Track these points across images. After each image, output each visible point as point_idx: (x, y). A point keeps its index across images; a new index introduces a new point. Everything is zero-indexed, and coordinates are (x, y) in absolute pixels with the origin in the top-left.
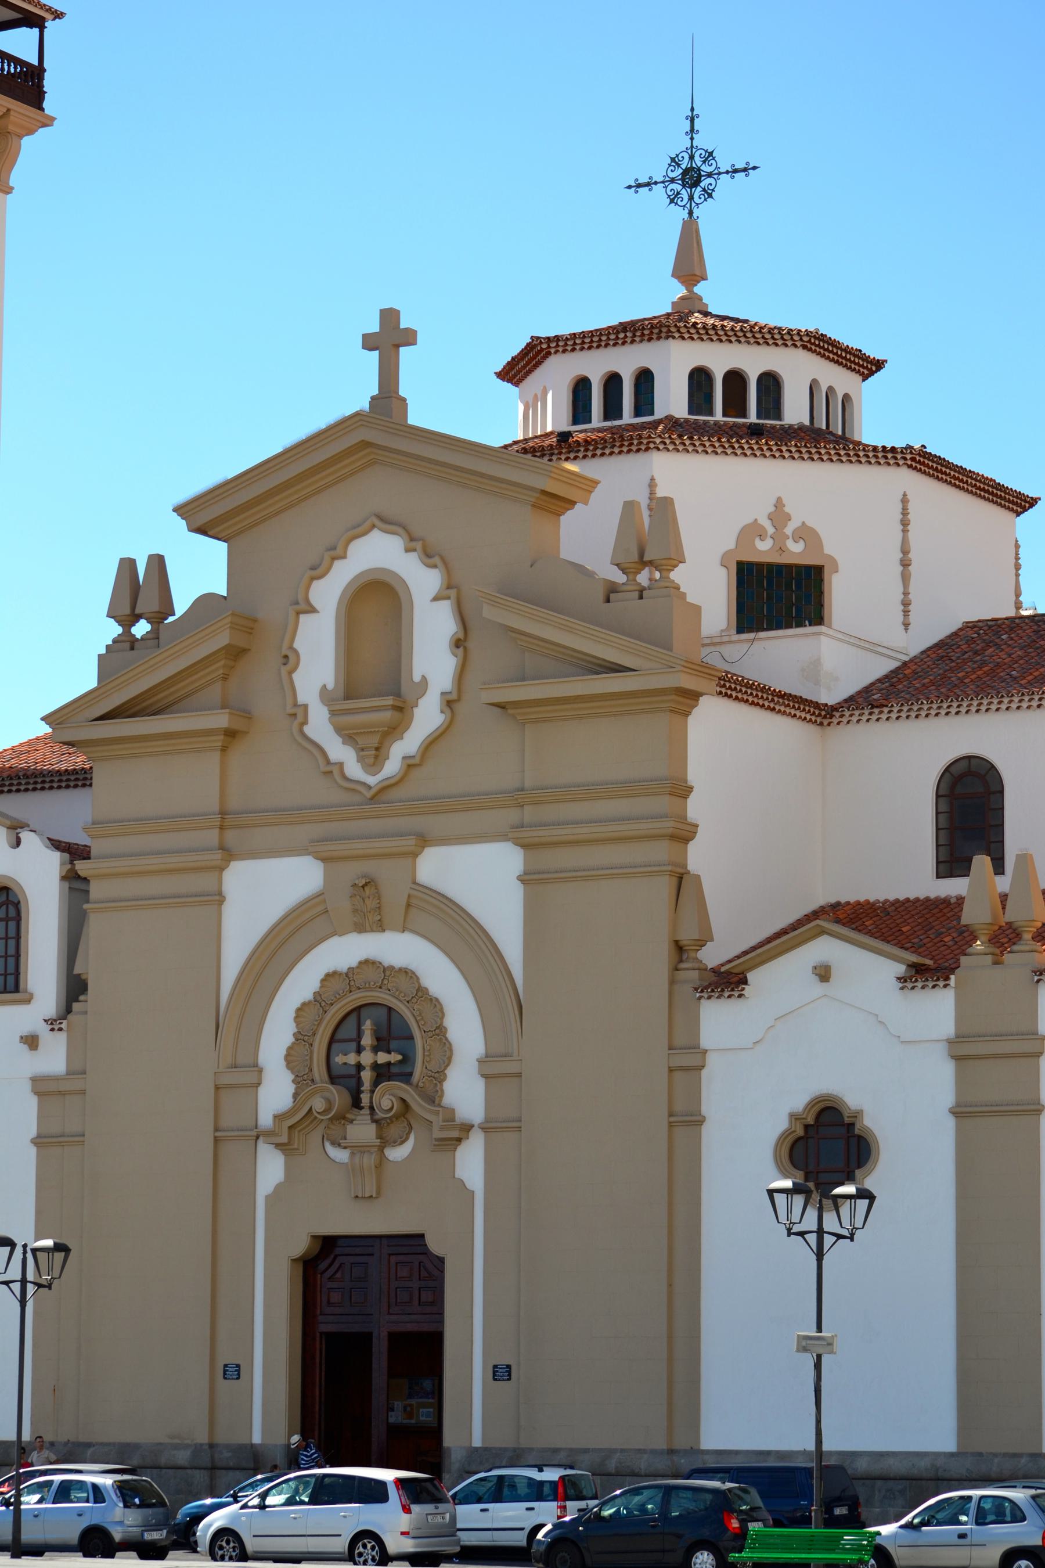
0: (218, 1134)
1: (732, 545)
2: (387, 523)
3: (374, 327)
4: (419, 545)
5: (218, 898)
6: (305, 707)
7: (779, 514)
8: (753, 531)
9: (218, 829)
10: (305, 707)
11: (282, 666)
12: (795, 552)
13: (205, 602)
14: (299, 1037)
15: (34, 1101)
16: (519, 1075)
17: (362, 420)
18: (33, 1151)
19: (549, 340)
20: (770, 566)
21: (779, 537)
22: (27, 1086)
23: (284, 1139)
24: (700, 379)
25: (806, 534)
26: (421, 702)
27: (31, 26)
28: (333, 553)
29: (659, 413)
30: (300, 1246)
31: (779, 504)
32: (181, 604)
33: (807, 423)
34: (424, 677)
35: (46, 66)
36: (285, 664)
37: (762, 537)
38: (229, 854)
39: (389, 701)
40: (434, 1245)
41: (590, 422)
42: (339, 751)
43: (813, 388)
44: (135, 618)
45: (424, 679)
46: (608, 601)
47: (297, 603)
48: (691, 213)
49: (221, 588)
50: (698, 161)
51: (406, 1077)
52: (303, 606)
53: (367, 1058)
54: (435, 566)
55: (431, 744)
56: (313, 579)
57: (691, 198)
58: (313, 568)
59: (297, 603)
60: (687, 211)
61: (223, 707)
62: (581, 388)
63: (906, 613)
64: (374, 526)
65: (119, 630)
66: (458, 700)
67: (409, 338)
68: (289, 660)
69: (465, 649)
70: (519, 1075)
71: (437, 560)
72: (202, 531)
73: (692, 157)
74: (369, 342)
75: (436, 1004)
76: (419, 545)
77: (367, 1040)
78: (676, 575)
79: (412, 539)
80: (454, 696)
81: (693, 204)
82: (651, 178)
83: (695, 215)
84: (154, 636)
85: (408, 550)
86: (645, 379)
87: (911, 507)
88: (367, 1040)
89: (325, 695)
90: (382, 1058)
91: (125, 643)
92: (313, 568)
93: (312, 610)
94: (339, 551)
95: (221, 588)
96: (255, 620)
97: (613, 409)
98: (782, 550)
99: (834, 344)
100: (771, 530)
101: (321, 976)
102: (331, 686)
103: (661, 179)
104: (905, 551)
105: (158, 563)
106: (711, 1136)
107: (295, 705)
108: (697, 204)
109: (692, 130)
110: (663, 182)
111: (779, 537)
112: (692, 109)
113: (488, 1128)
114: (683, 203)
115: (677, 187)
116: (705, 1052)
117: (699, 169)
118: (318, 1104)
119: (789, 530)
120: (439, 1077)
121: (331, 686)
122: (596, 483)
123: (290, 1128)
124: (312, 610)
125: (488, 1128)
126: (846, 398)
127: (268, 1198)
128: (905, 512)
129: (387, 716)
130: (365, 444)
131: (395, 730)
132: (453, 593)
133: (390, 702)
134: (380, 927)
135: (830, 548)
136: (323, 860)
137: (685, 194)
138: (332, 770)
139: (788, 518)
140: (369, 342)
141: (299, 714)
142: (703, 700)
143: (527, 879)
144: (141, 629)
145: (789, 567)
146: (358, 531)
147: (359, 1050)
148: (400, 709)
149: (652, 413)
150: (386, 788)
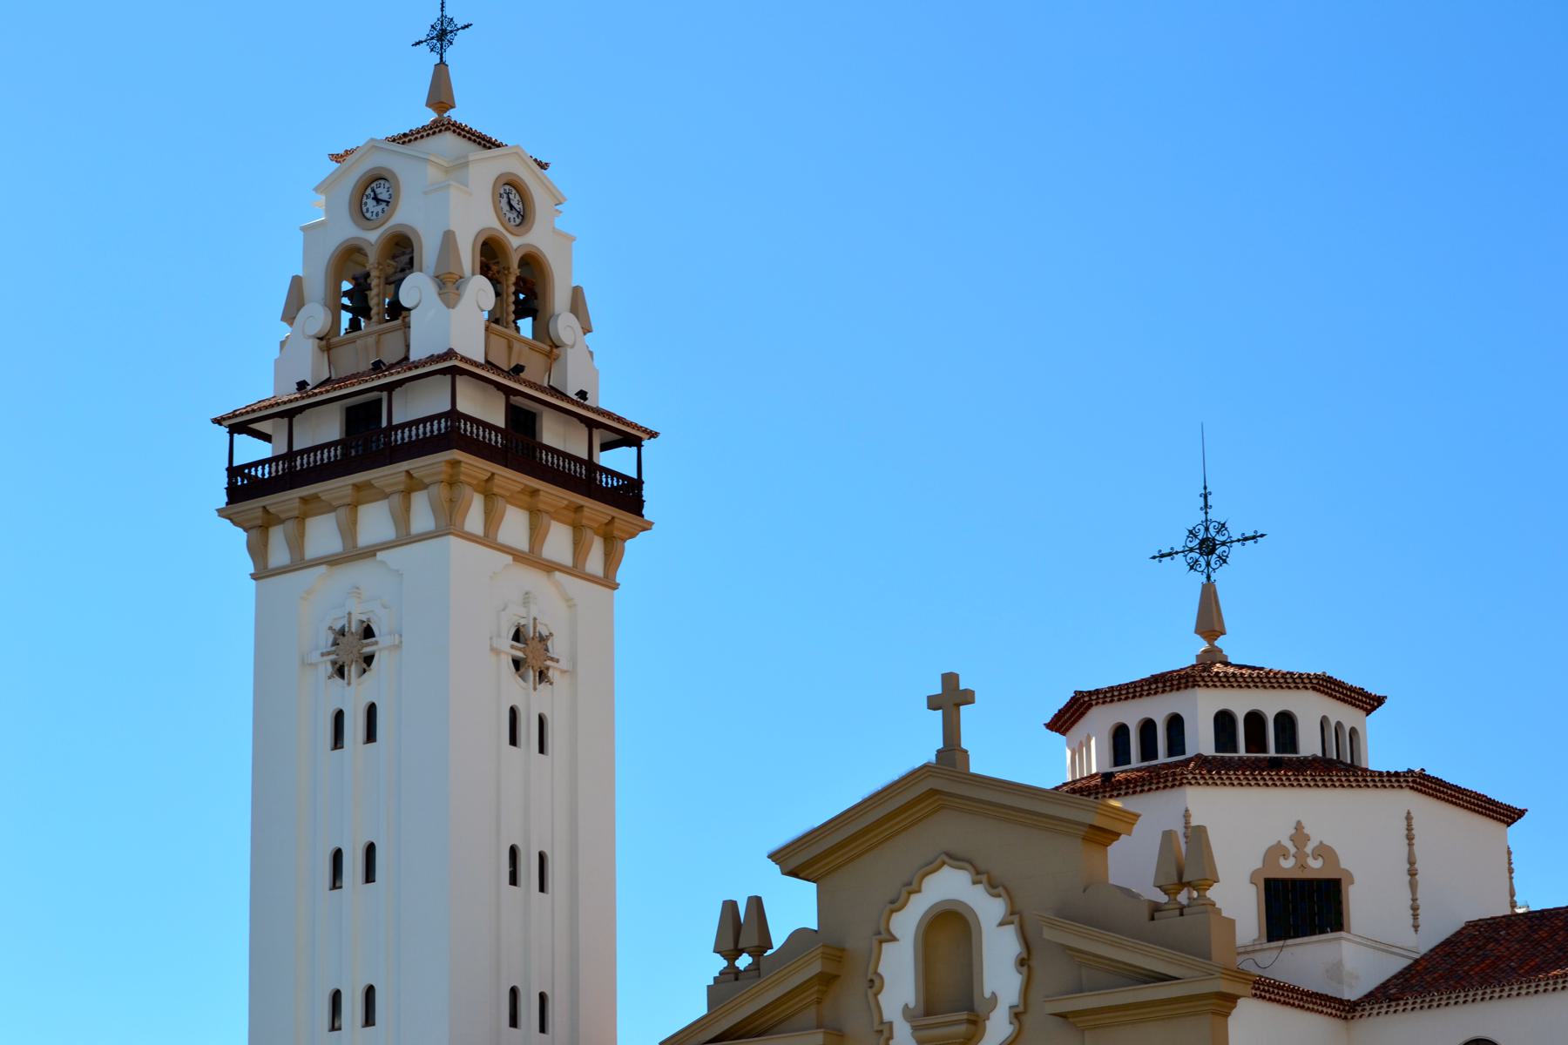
1: (1259, 865)
2: (957, 859)
3: (937, 689)
4: (984, 878)
6: (891, 1024)
7: (1299, 836)
8: (1277, 851)
12: (1316, 867)
13: (799, 936)
19: (1090, 693)
20: (1294, 881)
21: (1300, 856)
24: (1224, 721)
25: (1324, 851)
27: (630, 445)
28: (909, 888)
29: (1190, 753)
31: (1299, 826)
32: (778, 938)
33: (1320, 754)
34: (993, 993)
35: (644, 478)
36: (871, 987)
37: (1285, 856)
39: (964, 1016)
41: (1129, 763)
43: (1324, 722)
44: (738, 953)
45: (993, 993)
46: (1153, 918)
47: (879, 933)
48: (1209, 577)
49: (812, 924)
50: (1212, 532)
52: (882, 937)
54: (999, 896)
56: (893, 911)
57: (1208, 564)
58: (892, 902)
59: (879, 933)
60: (1205, 576)
61: (818, 1027)
62: (1120, 733)
63: (1415, 916)
64: (944, 863)
65: (724, 963)
66: (1024, 1012)
67: (968, 697)
68: (874, 983)
69: (1029, 968)
71: (1000, 890)
72: (794, 873)
73: (1207, 529)
74: (933, 703)
76: (984, 878)
78: (1212, 894)
79: (978, 873)
80: (1021, 1009)
81: (1211, 569)
82: (1172, 549)
83: (1212, 579)
84: (755, 968)
85: (975, 883)
86: (1176, 723)
87: (1414, 822)
91: (731, 974)
92: (892, 902)
93: (893, 939)
94: (914, 886)
95: (812, 924)
96: (843, 950)
97: (1149, 751)
98: (1303, 867)
99: (1340, 684)
100: (1293, 850)
102: (912, 1005)
103: (1182, 549)
104: (1412, 862)
105: (756, 903)
107: (882, 1023)
108: (1214, 569)
109: (1206, 505)
110: (1183, 552)
111: (1300, 856)
112: (1205, 488)
114: (1201, 569)
115: (1195, 555)
117: (1214, 539)
119: (1309, 849)
121: (912, 1005)
122: (1138, 816)
124: (893, 939)
126: (1353, 731)
128: (1409, 828)
129: (962, 1028)
130: (934, 792)
132: (1016, 918)
133: (965, 1017)
135: (1344, 864)
137: (1202, 561)
139: (1308, 838)
140: (933, 703)
142: (1240, 1002)
144: (744, 961)
145: (1311, 881)
146: (931, 867)
149: (1184, 753)
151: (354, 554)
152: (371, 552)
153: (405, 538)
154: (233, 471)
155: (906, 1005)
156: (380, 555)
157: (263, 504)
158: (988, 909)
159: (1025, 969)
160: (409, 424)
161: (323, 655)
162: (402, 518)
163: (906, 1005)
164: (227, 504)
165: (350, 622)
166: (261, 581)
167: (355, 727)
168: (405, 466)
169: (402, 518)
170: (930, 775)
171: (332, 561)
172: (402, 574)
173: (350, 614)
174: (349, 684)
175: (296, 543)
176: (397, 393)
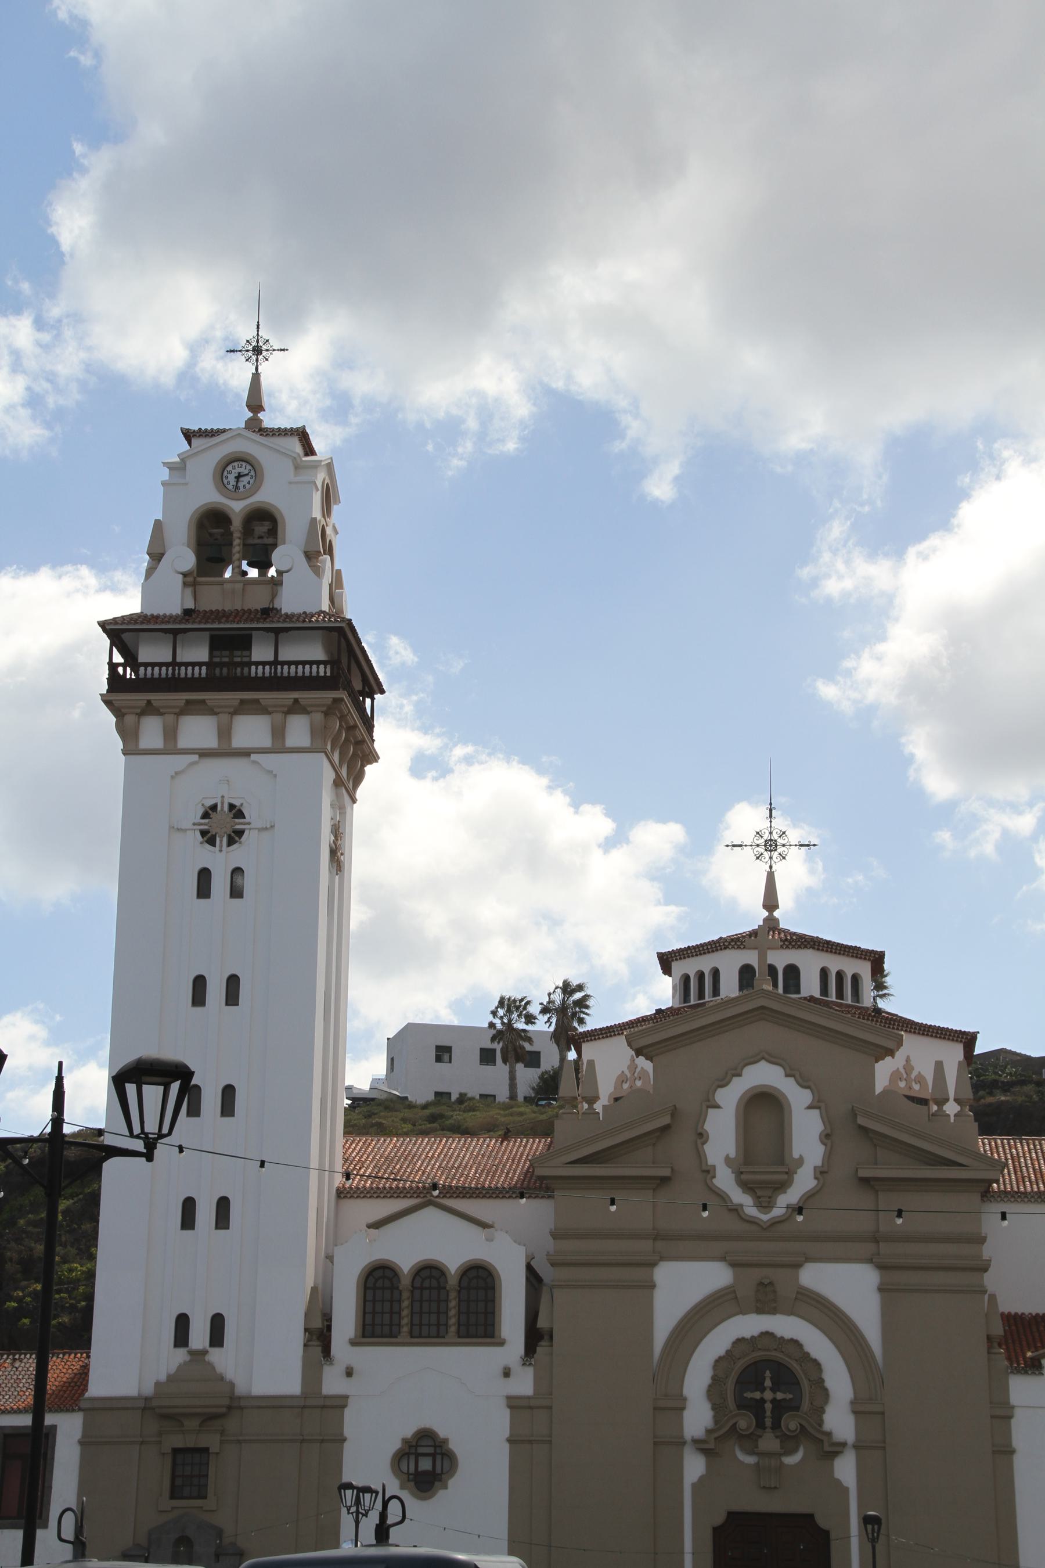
0: (656, 1440)
5: (653, 1286)
6: (714, 1167)
9: (652, 1240)
10: (714, 1167)
11: (698, 1140)
14: (715, 1378)
15: (508, 1411)
16: (883, 1413)
17: (762, 993)
18: (507, 1445)
22: (503, 1402)
23: (711, 1446)
26: (799, 1171)
30: (719, 1519)
38: (662, 1258)
40: (822, 1522)
42: (739, 1197)
45: (801, 1155)
47: (709, 1101)
51: (797, 1408)
53: (768, 1395)
55: (810, 1196)
68: (702, 1136)
70: (883, 1413)
75: (817, 1364)
77: (768, 1383)
80: (825, 1169)
88: (768, 1383)
89: (728, 1160)
90: (780, 1396)
93: (718, 1107)
101: (733, 1339)
106: (1020, 1463)
113: (856, 1447)
116: (1013, 1407)
118: (742, 1424)
120: (822, 1411)
121: (732, 1154)
123: (716, 1439)
124: (717, 1107)
125: (856, 1447)
127: (694, 1485)
129: (786, 1177)
130: (763, 1007)
131: (782, 1186)
134: (773, 1311)
136: (733, 1265)
138: (736, 1210)
141: (709, 1172)
143: (881, 1289)
147: (763, 1390)
148: (787, 1173)
150: (776, 1222)
151: (225, 751)
152: (245, 753)
153: (279, 746)
154: (112, 667)
155: (728, 1155)
156: (253, 757)
157: (149, 698)
158: (798, 1097)
159: (829, 1142)
160: (289, 663)
161: (194, 824)
162: (278, 733)
163: (728, 1155)
164: (108, 691)
165: (222, 803)
166: (127, 756)
167: (220, 884)
168: (295, 695)
169: (278, 733)
170: (762, 996)
171: (205, 754)
172: (275, 776)
173: (223, 797)
174: (221, 851)
175: (171, 734)
176: (281, 636)
